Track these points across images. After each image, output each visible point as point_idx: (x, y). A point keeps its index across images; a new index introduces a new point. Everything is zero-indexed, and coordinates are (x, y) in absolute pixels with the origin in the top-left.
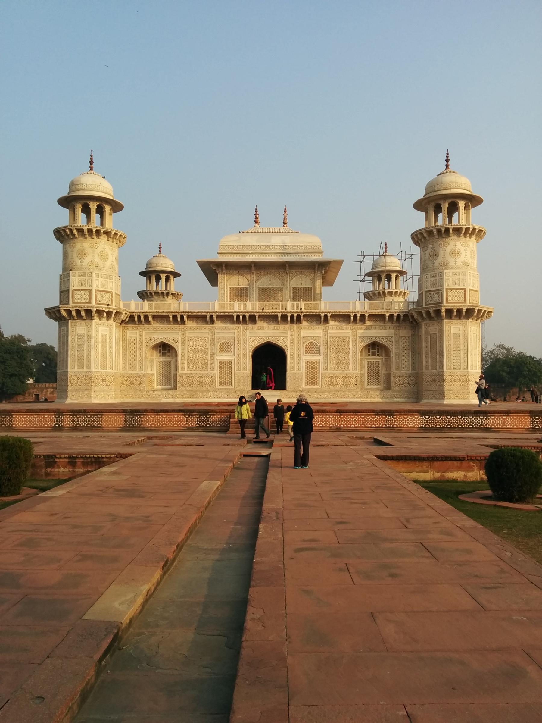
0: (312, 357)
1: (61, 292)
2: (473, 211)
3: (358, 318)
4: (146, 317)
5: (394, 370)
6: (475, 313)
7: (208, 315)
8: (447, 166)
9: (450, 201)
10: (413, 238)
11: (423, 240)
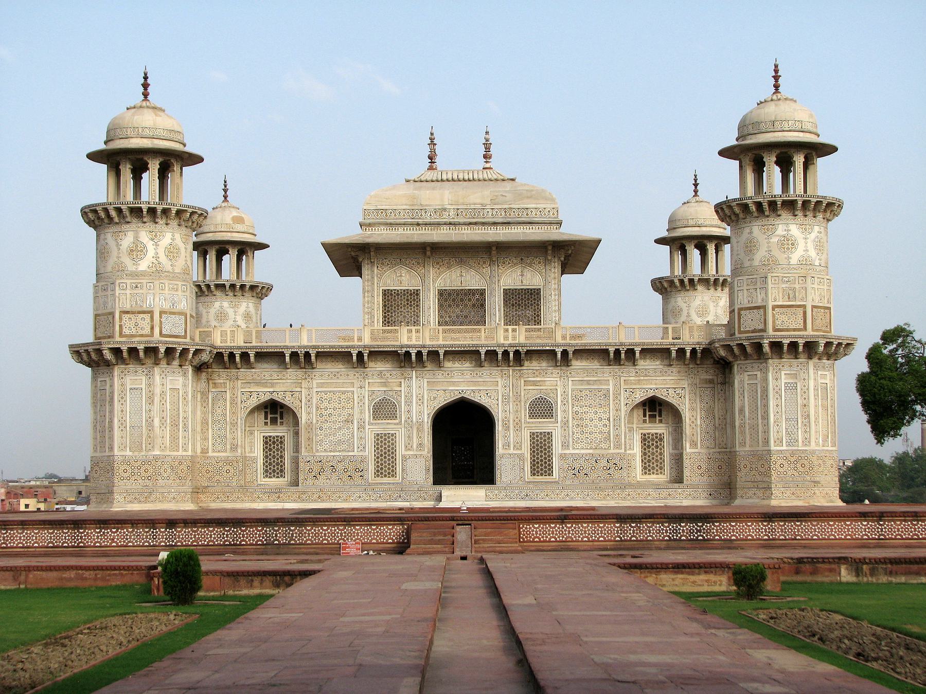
0: (543, 425)
1: (96, 316)
2: (821, 163)
3: (623, 356)
4: (245, 356)
5: (688, 449)
6: (821, 349)
7: (354, 353)
8: (777, 87)
9: (778, 151)
10: (717, 212)
11: (733, 217)
